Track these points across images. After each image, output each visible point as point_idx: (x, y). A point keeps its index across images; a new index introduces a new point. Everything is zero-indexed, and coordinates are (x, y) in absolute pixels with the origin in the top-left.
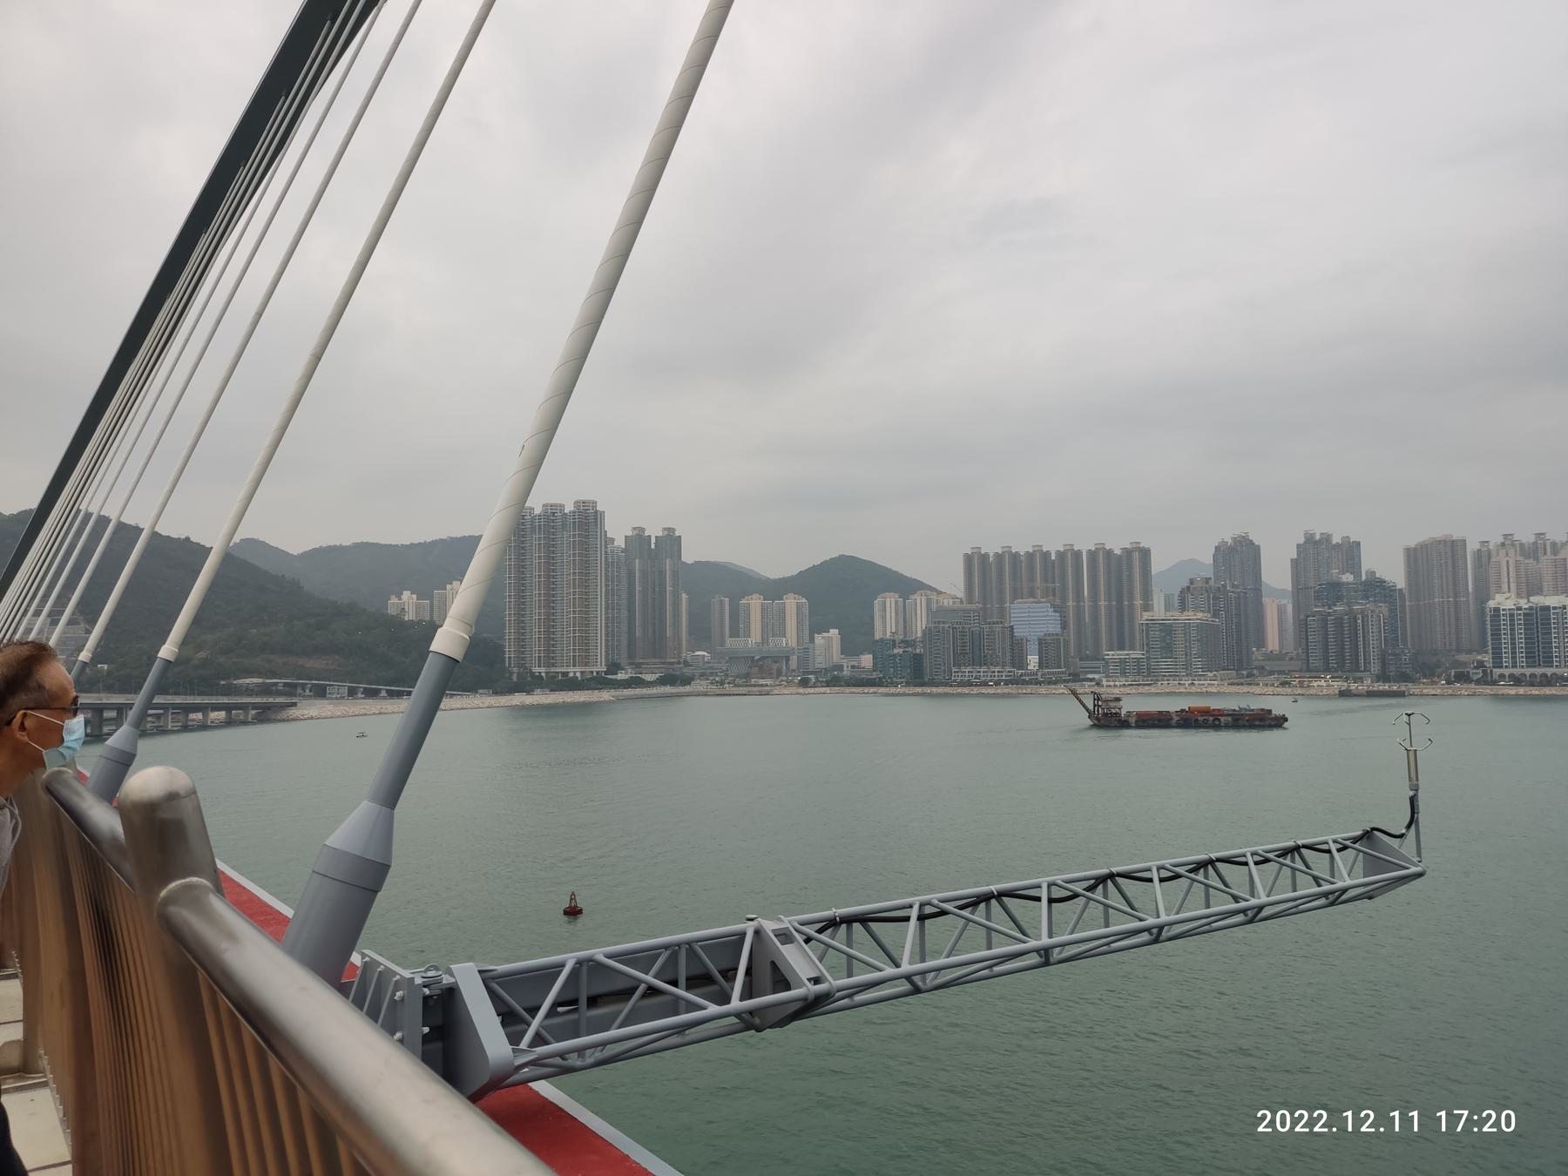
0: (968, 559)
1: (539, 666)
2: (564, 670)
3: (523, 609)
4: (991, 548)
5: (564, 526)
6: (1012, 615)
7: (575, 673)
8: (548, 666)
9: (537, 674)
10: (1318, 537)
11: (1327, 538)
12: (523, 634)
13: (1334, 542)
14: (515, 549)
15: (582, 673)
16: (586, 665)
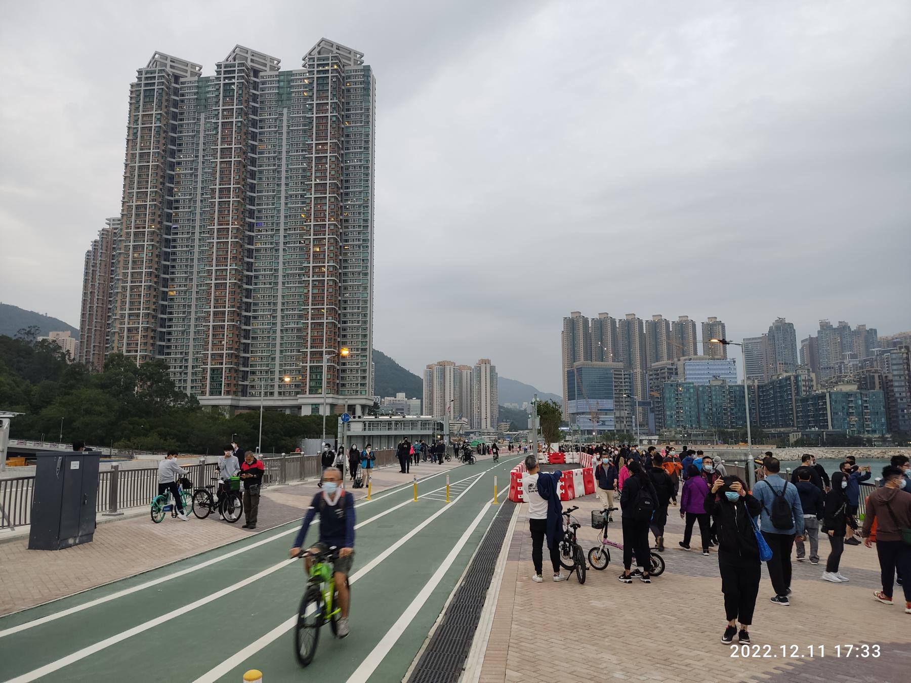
0: (573, 325)
1: (215, 391)
2: (275, 401)
3: (166, 269)
4: (591, 314)
5: (282, 98)
6: (687, 372)
7: (316, 407)
8: (235, 393)
9: (209, 410)
10: (835, 325)
11: (844, 328)
12: (163, 323)
13: (852, 330)
14: (158, 133)
15: (333, 406)
16: (338, 393)
